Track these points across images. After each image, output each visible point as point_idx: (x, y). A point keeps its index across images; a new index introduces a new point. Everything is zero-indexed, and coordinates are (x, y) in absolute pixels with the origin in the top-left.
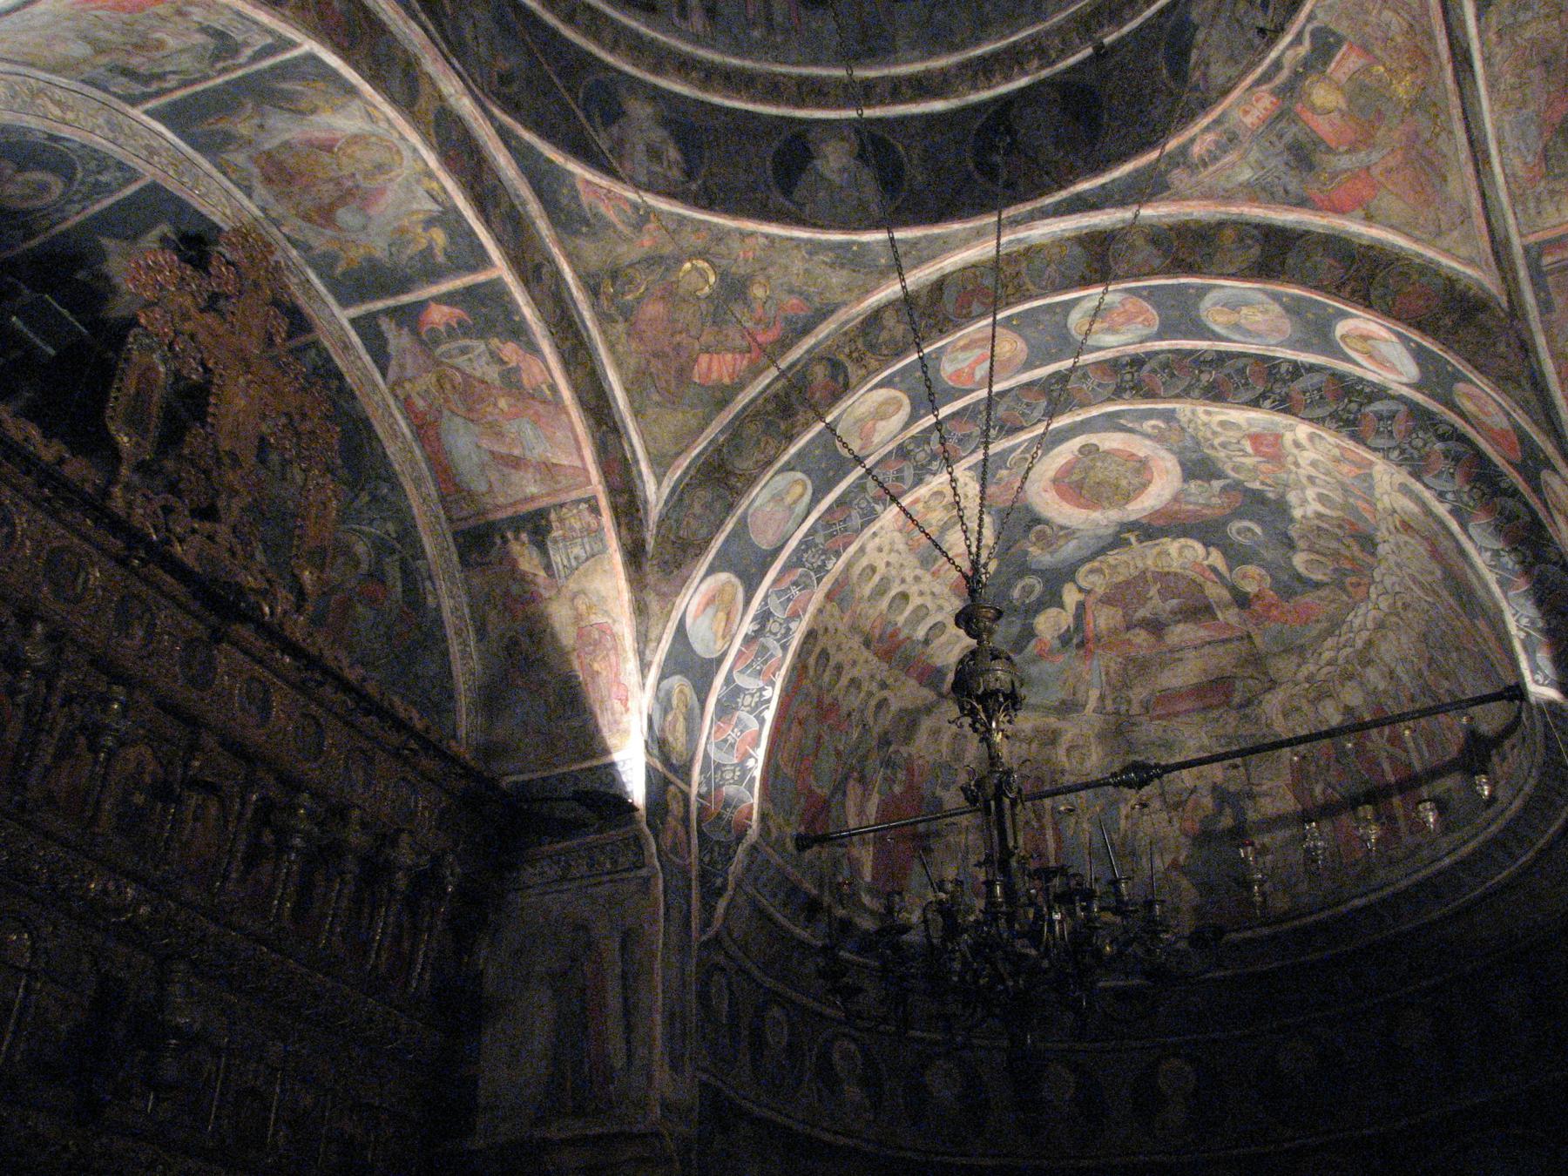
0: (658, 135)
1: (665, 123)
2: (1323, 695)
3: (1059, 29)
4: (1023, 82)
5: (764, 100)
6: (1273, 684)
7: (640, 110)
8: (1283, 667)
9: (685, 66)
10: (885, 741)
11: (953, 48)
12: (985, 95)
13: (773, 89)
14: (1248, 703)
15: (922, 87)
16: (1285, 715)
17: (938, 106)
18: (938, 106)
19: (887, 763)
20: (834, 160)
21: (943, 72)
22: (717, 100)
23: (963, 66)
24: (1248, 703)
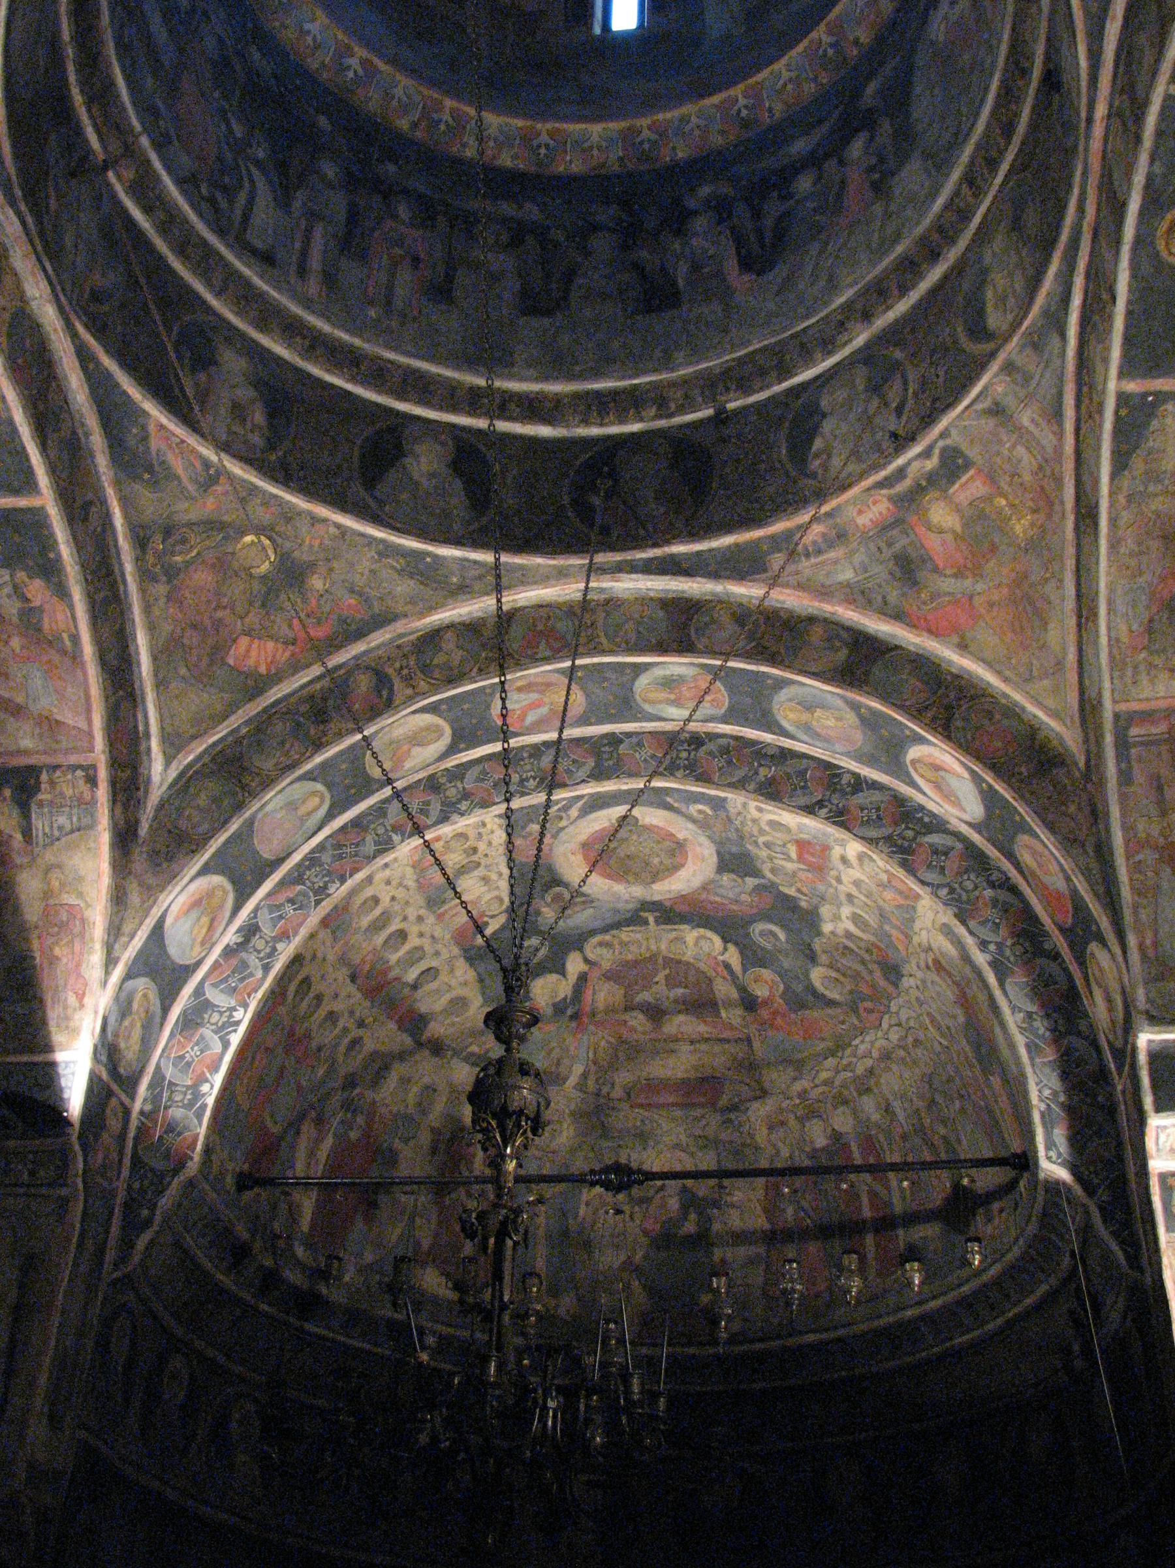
0: (245, 393)
1: (257, 383)
2: (812, 1113)
3: (685, 382)
4: (636, 427)
5: (365, 383)
6: (763, 1094)
7: (233, 363)
8: (776, 1078)
9: (292, 329)
10: (351, 1082)
11: (571, 377)
12: (595, 431)
13: (379, 375)
14: (734, 1108)
15: (533, 408)
16: (771, 1128)
17: (545, 431)
18: (545, 431)
19: (348, 1105)
20: (425, 463)
21: (557, 400)
22: (316, 371)
23: (577, 396)
24: (734, 1108)
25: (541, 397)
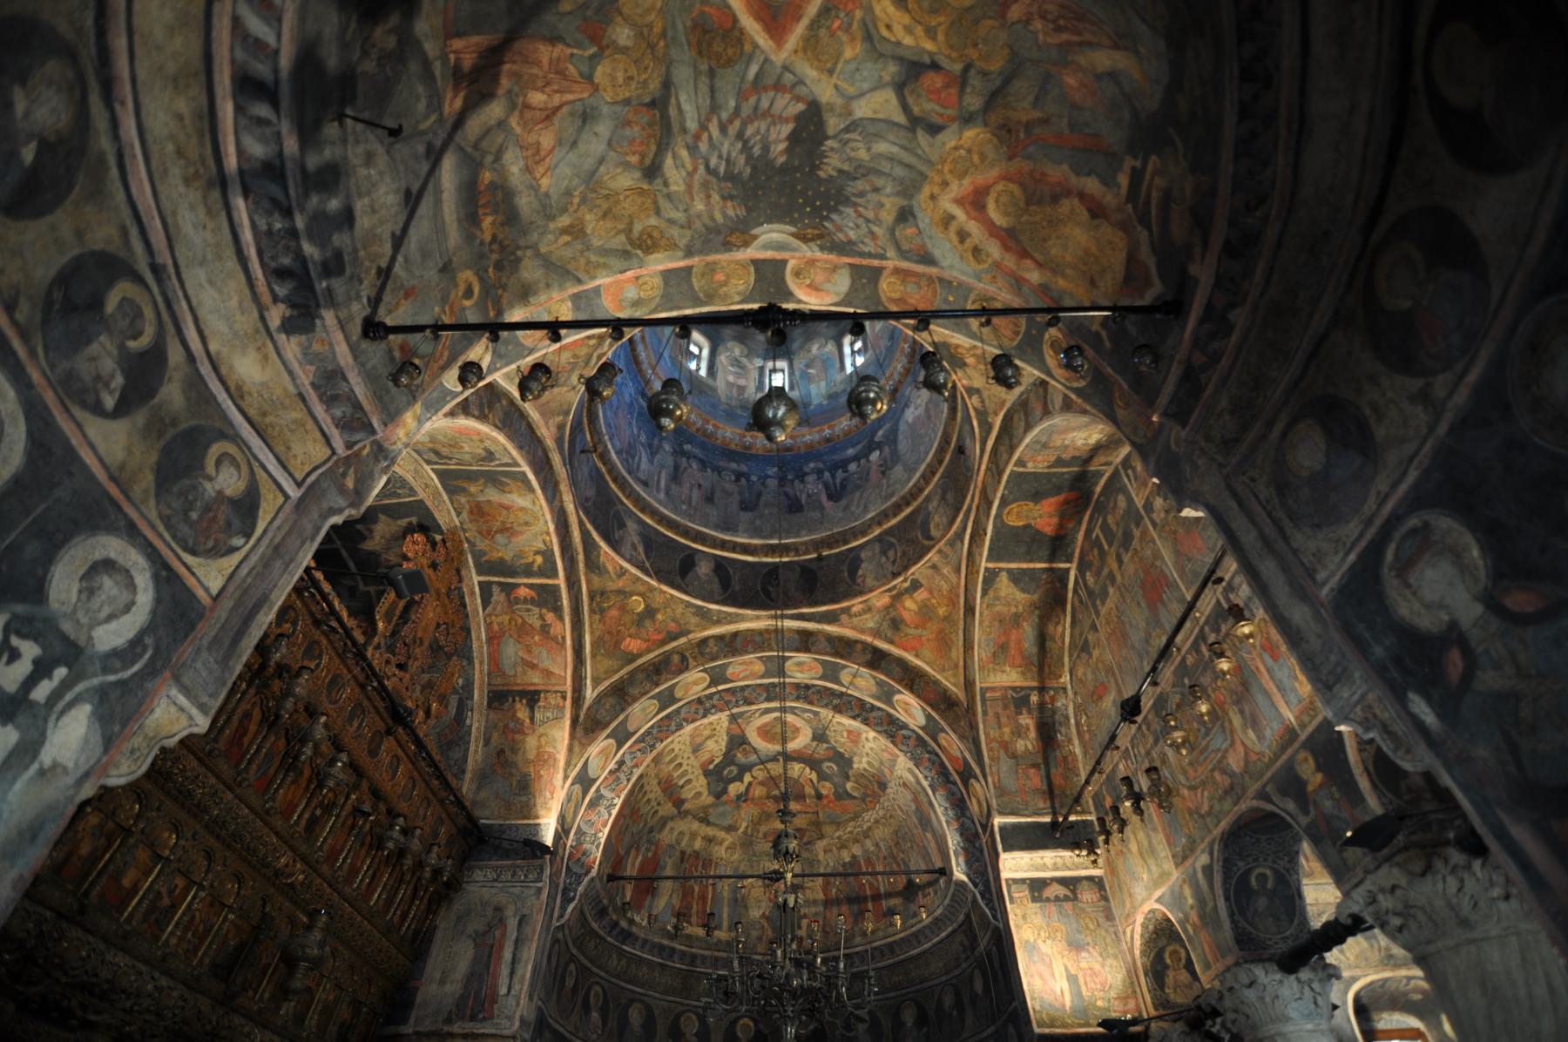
0: (636, 539)
1: (641, 534)
2: (843, 846)
3: (805, 543)
4: (785, 559)
5: (681, 536)
6: (822, 837)
7: (631, 526)
8: (828, 830)
9: (654, 513)
12: (770, 560)
13: (686, 533)
14: (809, 843)
15: (746, 549)
17: (750, 559)
18: (750, 559)
19: (649, 841)
20: (704, 569)
21: (756, 546)
24: (809, 843)
25: (749, 545)
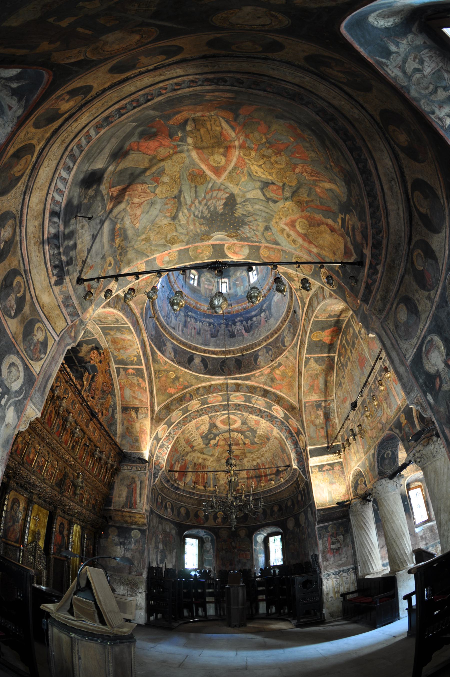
1: (173, 348)
2: (254, 460)
3: (237, 349)
4: (229, 356)
6: (246, 457)
7: (169, 345)
8: (248, 455)
9: (177, 340)
10: (183, 456)
11: (220, 348)
12: (223, 357)
13: (190, 347)
15: (213, 353)
19: (182, 459)
20: (197, 361)
21: (217, 351)
23: (220, 351)
25: (215, 351)
